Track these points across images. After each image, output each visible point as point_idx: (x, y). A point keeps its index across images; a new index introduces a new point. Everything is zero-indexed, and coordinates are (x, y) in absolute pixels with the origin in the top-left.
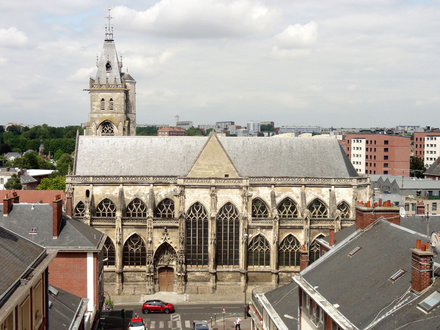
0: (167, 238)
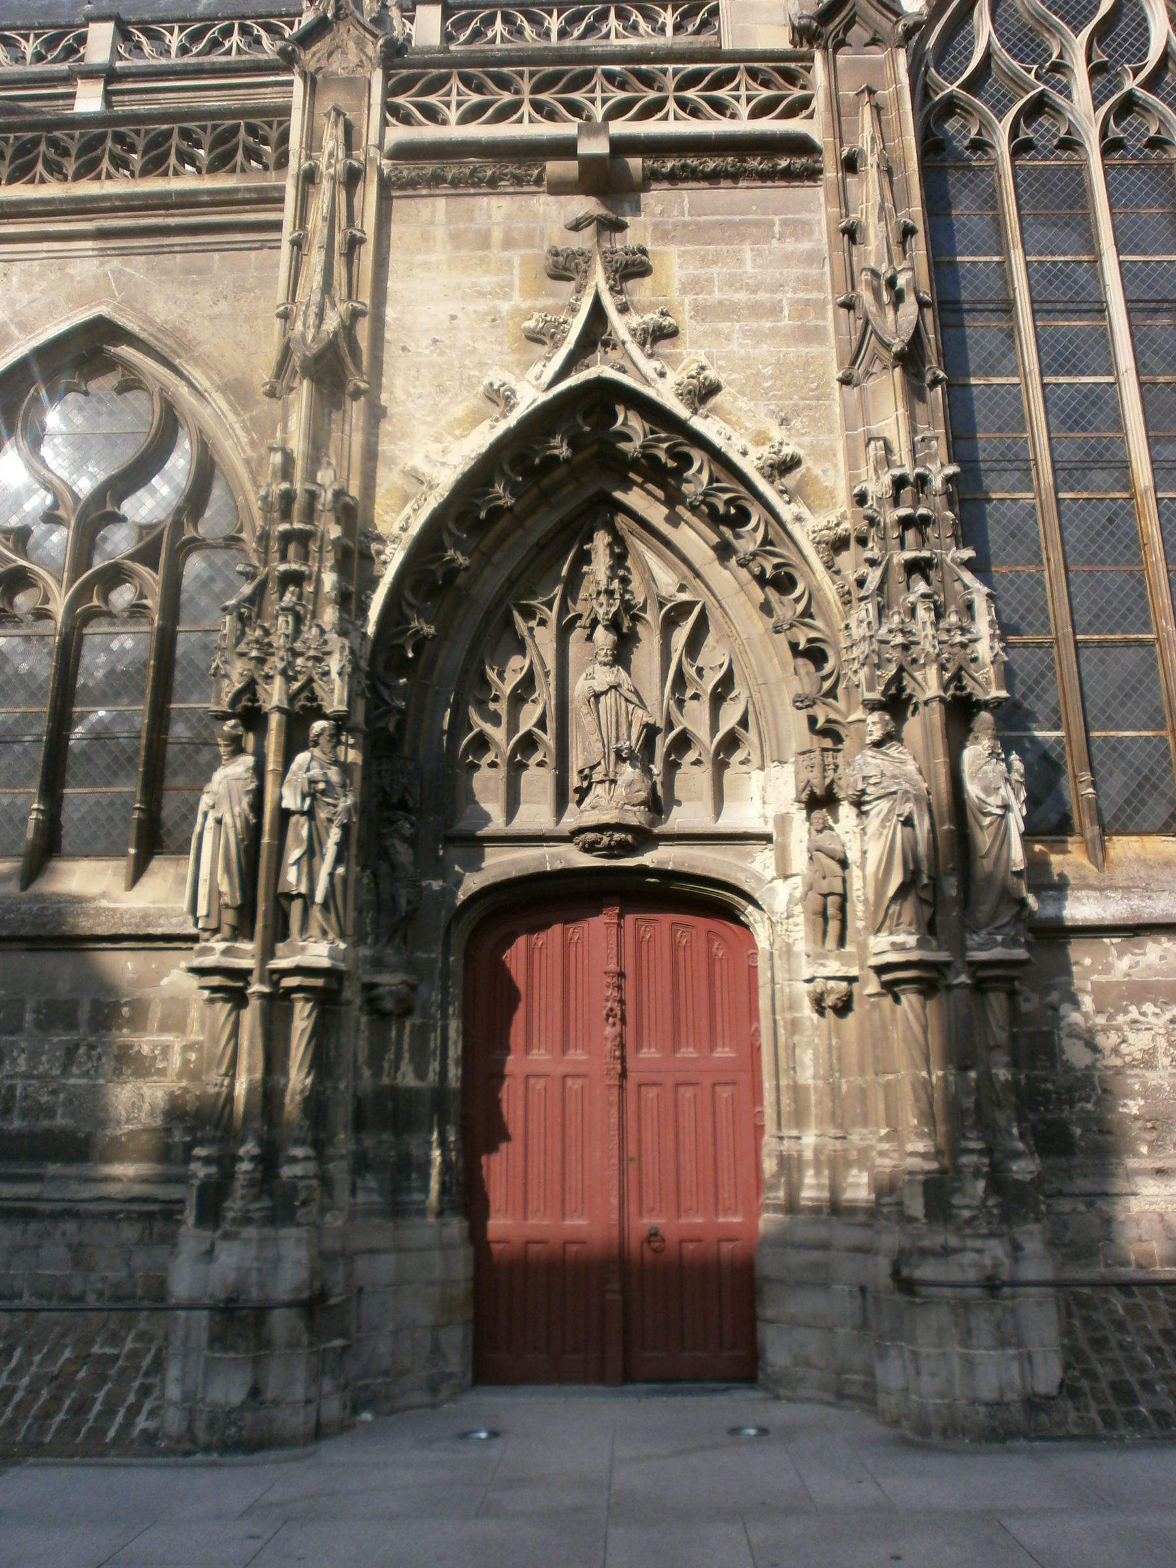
0: (620, 325)
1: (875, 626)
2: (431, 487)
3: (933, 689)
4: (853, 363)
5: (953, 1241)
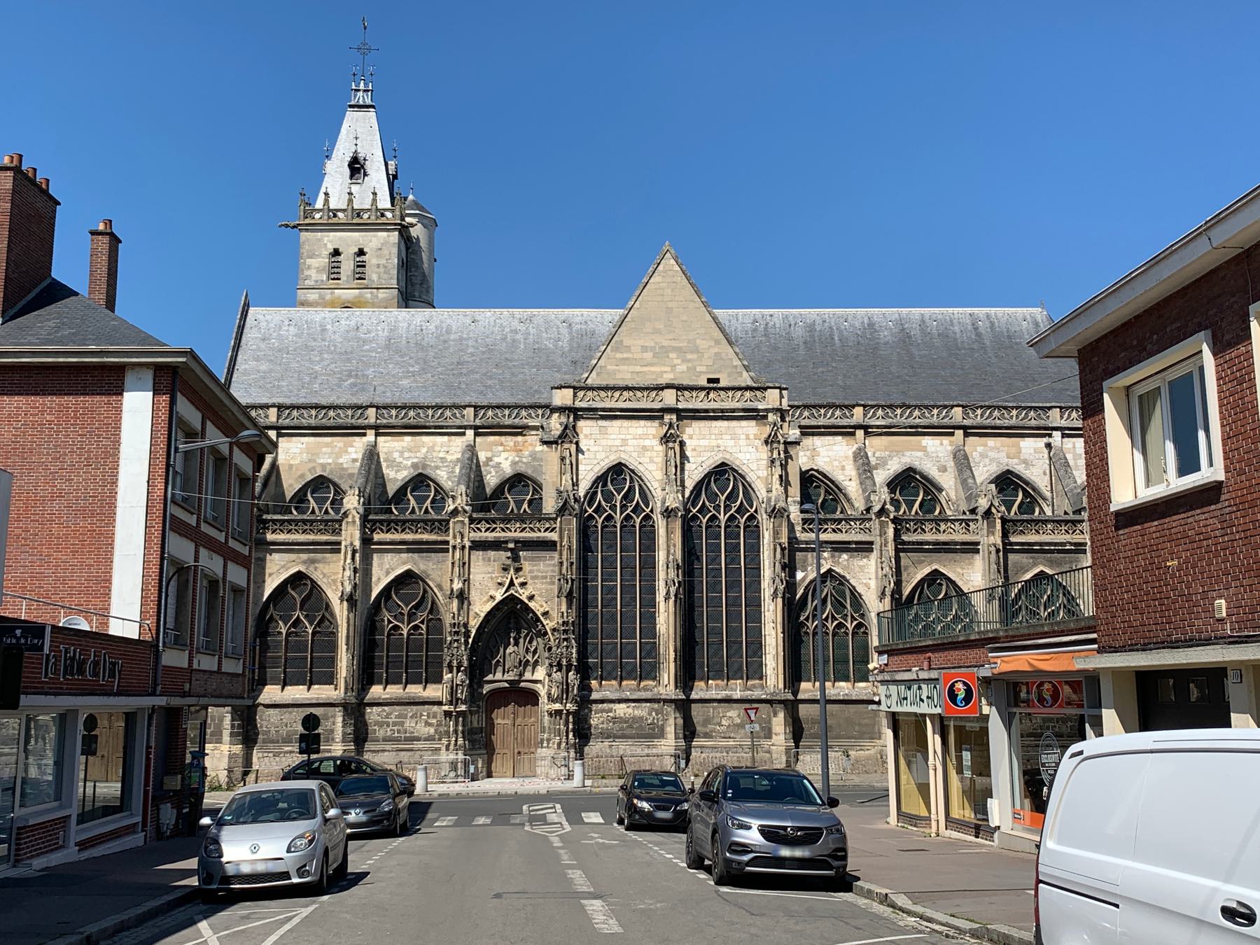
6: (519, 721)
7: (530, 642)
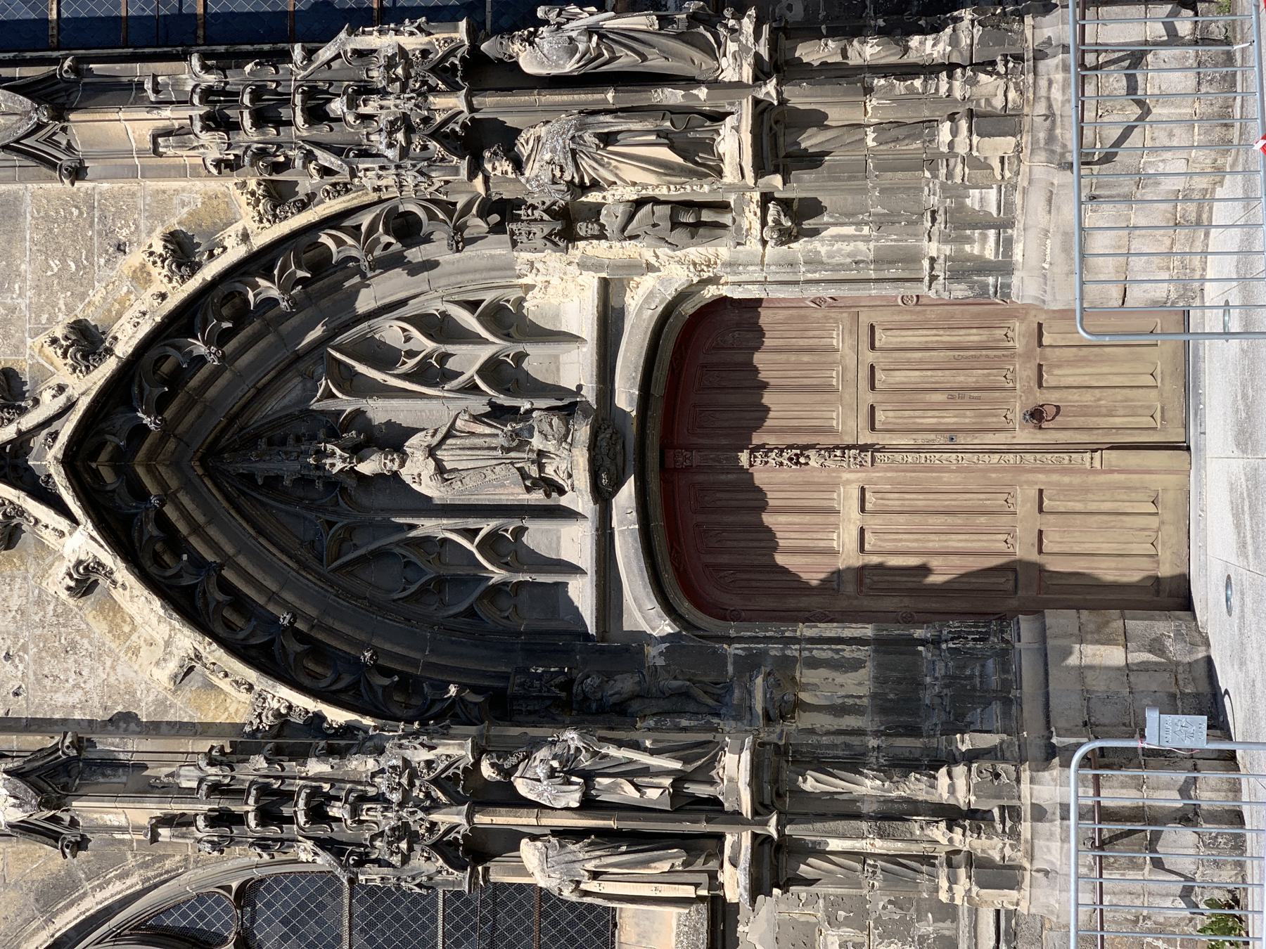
1: (382, 162)
2: (198, 657)
3: (457, 102)
4: (53, 166)
5: (1041, 108)
6: (850, 427)
7: (385, 357)
